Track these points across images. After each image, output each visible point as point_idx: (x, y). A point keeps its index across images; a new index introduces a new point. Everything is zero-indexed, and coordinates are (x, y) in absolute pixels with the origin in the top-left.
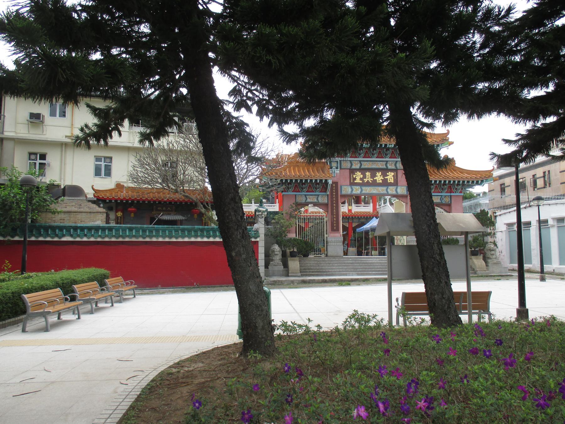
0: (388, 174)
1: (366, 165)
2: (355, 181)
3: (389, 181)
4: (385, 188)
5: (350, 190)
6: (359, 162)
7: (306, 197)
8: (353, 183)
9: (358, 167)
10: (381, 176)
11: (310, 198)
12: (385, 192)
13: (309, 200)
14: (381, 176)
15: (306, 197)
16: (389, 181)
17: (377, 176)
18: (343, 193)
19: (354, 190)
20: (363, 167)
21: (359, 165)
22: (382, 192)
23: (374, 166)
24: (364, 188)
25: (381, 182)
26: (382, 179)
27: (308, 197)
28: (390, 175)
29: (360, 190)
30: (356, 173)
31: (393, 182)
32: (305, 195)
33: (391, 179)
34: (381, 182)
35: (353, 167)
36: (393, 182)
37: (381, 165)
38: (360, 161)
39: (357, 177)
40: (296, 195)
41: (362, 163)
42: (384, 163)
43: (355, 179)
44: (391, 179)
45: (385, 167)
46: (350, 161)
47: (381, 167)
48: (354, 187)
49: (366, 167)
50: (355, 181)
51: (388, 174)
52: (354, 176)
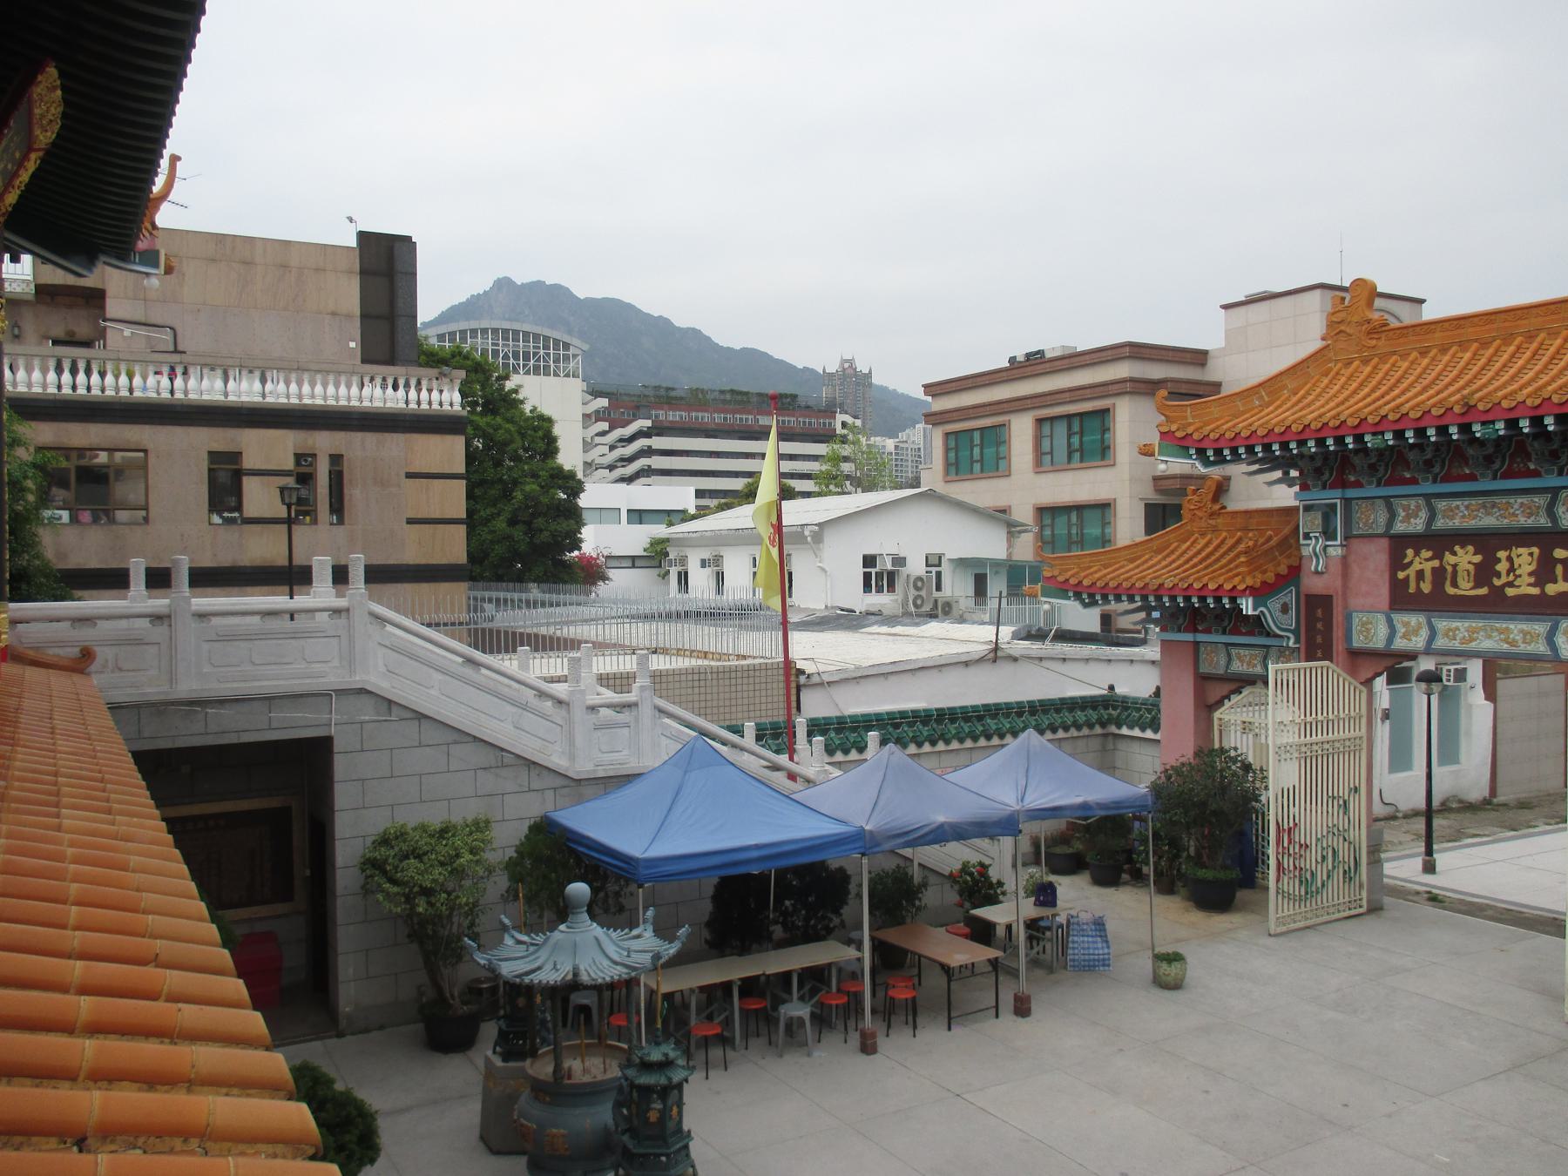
1: (1459, 515)
4: (1540, 628)
5: (1382, 630)
6: (1421, 501)
7: (1229, 655)
8: (1402, 598)
9: (1418, 525)
11: (1239, 658)
12: (1541, 648)
13: (1237, 667)
15: (1229, 655)
18: (1358, 642)
19: (1401, 630)
20: (1440, 524)
21: (1423, 515)
22: (1523, 648)
23: (1489, 521)
24: (1442, 624)
27: (1234, 651)
29: (1424, 633)
32: (1227, 645)
35: (1400, 527)
37: (1521, 513)
38: (1428, 497)
40: (1196, 644)
41: (1441, 505)
42: (1540, 501)
45: (1543, 521)
46: (1387, 499)
47: (1523, 521)
48: (1398, 618)
49: (1456, 523)
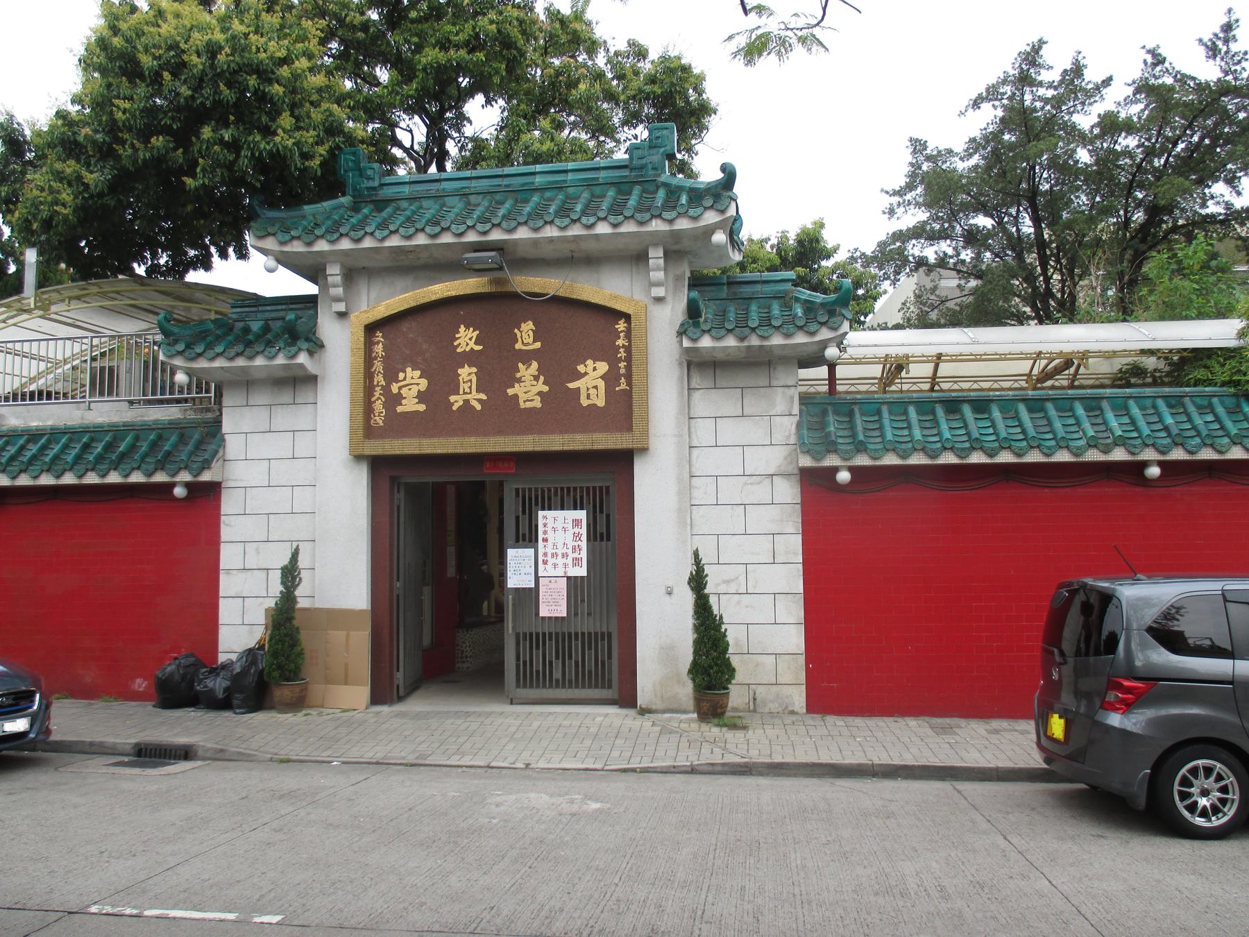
0: (581, 368)
2: (399, 409)
3: (585, 402)
10: (536, 378)
14: (536, 378)
16: (585, 402)
17: (519, 381)
25: (537, 403)
26: (540, 394)
28: (592, 374)
30: (401, 376)
31: (601, 403)
33: (592, 391)
34: (537, 403)
36: (601, 403)
39: (404, 391)
43: (398, 398)
44: (592, 391)
50: (399, 409)
51: (581, 368)
52: (395, 388)
